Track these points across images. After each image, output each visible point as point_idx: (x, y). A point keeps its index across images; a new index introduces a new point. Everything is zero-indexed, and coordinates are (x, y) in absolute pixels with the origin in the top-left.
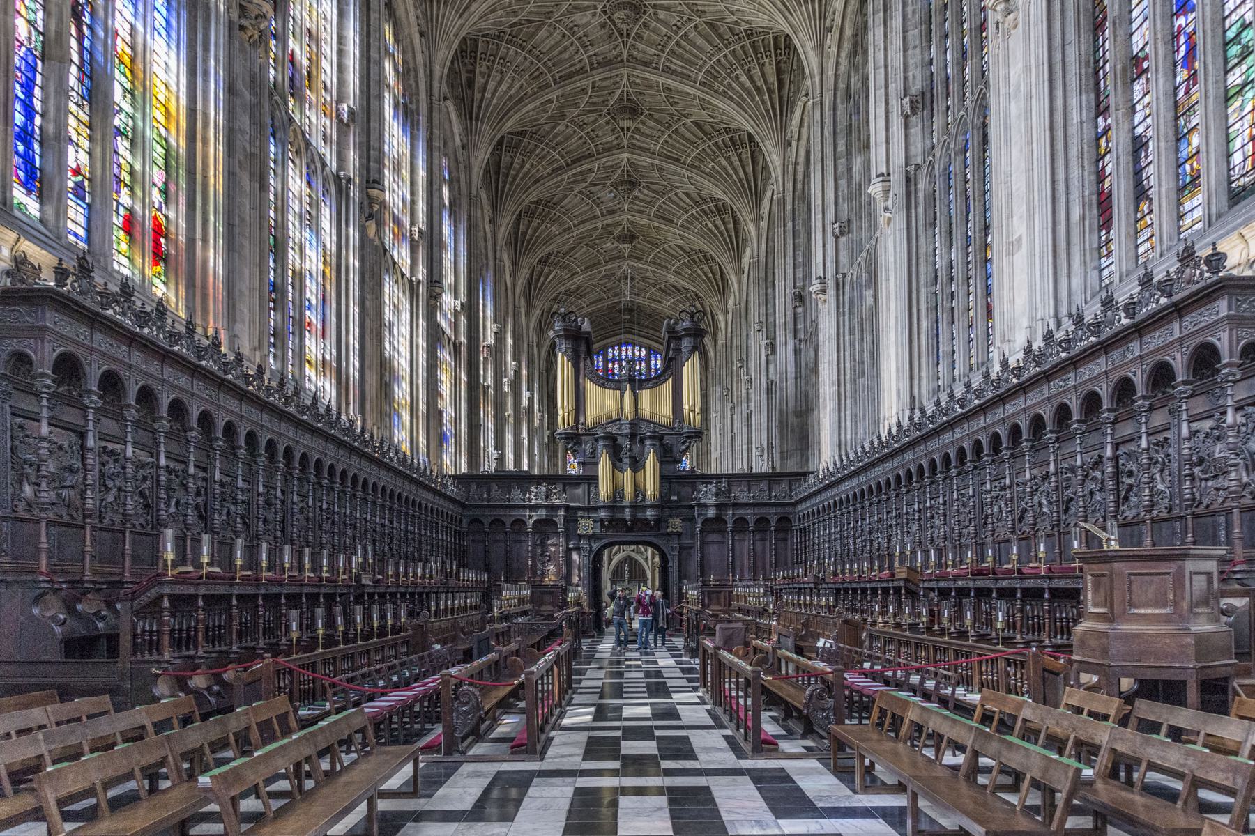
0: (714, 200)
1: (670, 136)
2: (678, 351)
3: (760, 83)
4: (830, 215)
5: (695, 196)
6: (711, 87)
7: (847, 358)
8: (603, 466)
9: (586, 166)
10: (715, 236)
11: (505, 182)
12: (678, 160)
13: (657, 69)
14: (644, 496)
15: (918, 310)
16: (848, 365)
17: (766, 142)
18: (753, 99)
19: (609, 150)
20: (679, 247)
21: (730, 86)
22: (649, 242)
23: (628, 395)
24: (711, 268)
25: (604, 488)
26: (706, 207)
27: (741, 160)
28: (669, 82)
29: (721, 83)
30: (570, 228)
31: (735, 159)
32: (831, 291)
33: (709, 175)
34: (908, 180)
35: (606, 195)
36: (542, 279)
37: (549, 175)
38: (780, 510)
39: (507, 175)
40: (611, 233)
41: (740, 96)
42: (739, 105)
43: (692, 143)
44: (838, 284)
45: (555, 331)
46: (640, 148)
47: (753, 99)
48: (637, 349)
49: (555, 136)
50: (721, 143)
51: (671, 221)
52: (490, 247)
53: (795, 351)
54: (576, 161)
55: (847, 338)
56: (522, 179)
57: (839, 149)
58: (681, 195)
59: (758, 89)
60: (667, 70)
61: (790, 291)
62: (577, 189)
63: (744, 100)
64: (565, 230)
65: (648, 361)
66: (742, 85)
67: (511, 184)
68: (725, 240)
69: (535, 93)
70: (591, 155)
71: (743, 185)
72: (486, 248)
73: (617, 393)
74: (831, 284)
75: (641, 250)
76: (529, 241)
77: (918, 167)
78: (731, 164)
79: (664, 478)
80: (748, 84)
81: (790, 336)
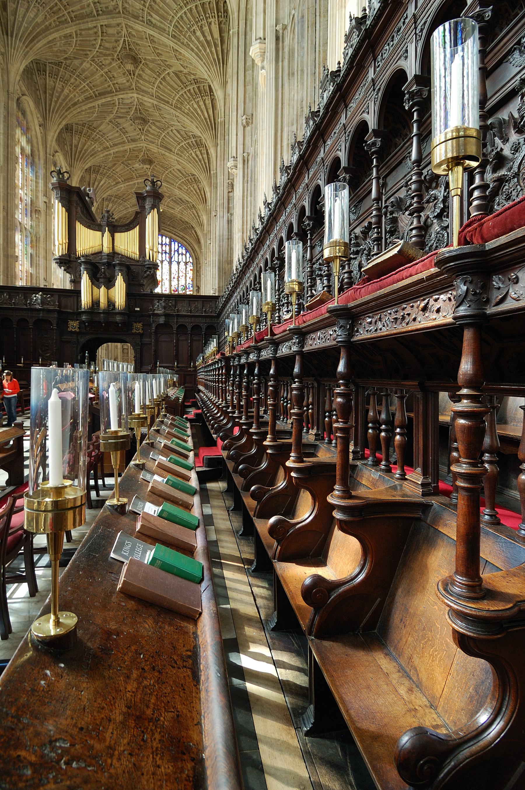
0: (194, 136)
1: (160, 82)
2: (143, 208)
3: (209, 38)
4: (241, 112)
5: (183, 133)
6: (179, 40)
7: (249, 213)
8: (85, 280)
9: (109, 99)
10: (197, 162)
11: (51, 100)
12: (168, 102)
13: (144, 22)
14: (114, 306)
15: (282, 147)
16: (249, 218)
17: (215, 83)
18: (205, 50)
19: (124, 90)
20: (179, 170)
21: (191, 40)
22: (162, 166)
23: (107, 234)
24: (198, 186)
25: (85, 299)
26: (190, 141)
27: (205, 104)
28: (152, 33)
29: (185, 36)
30: (108, 148)
31: (201, 103)
32: (240, 165)
33: (188, 114)
34: (277, 38)
35: (127, 125)
36: (96, 183)
37: (83, 101)
38: (208, 320)
39: (52, 95)
40: (137, 157)
41: (197, 48)
42: (197, 54)
43: (175, 89)
44: (244, 161)
45: (53, 184)
46: (143, 91)
47: (205, 50)
48: (164, 238)
49: (84, 71)
50: (192, 91)
51: (171, 150)
52: (40, 143)
53: (228, 221)
54: (102, 94)
55: (249, 199)
56: (64, 100)
57: (248, 64)
58: (175, 131)
59: (208, 42)
60: (150, 23)
61: (226, 181)
62: (108, 119)
63: (200, 51)
64: (104, 148)
65: (170, 245)
66: (198, 39)
67: (56, 102)
68: (202, 165)
69: (57, 26)
70: (111, 92)
71: (207, 122)
72: (38, 144)
73: (99, 234)
74: (240, 160)
75: (157, 171)
76: (80, 152)
77: (285, 28)
78: (199, 107)
79: (129, 295)
80: (202, 38)
81: (226, 210)
